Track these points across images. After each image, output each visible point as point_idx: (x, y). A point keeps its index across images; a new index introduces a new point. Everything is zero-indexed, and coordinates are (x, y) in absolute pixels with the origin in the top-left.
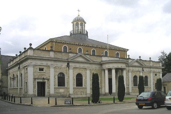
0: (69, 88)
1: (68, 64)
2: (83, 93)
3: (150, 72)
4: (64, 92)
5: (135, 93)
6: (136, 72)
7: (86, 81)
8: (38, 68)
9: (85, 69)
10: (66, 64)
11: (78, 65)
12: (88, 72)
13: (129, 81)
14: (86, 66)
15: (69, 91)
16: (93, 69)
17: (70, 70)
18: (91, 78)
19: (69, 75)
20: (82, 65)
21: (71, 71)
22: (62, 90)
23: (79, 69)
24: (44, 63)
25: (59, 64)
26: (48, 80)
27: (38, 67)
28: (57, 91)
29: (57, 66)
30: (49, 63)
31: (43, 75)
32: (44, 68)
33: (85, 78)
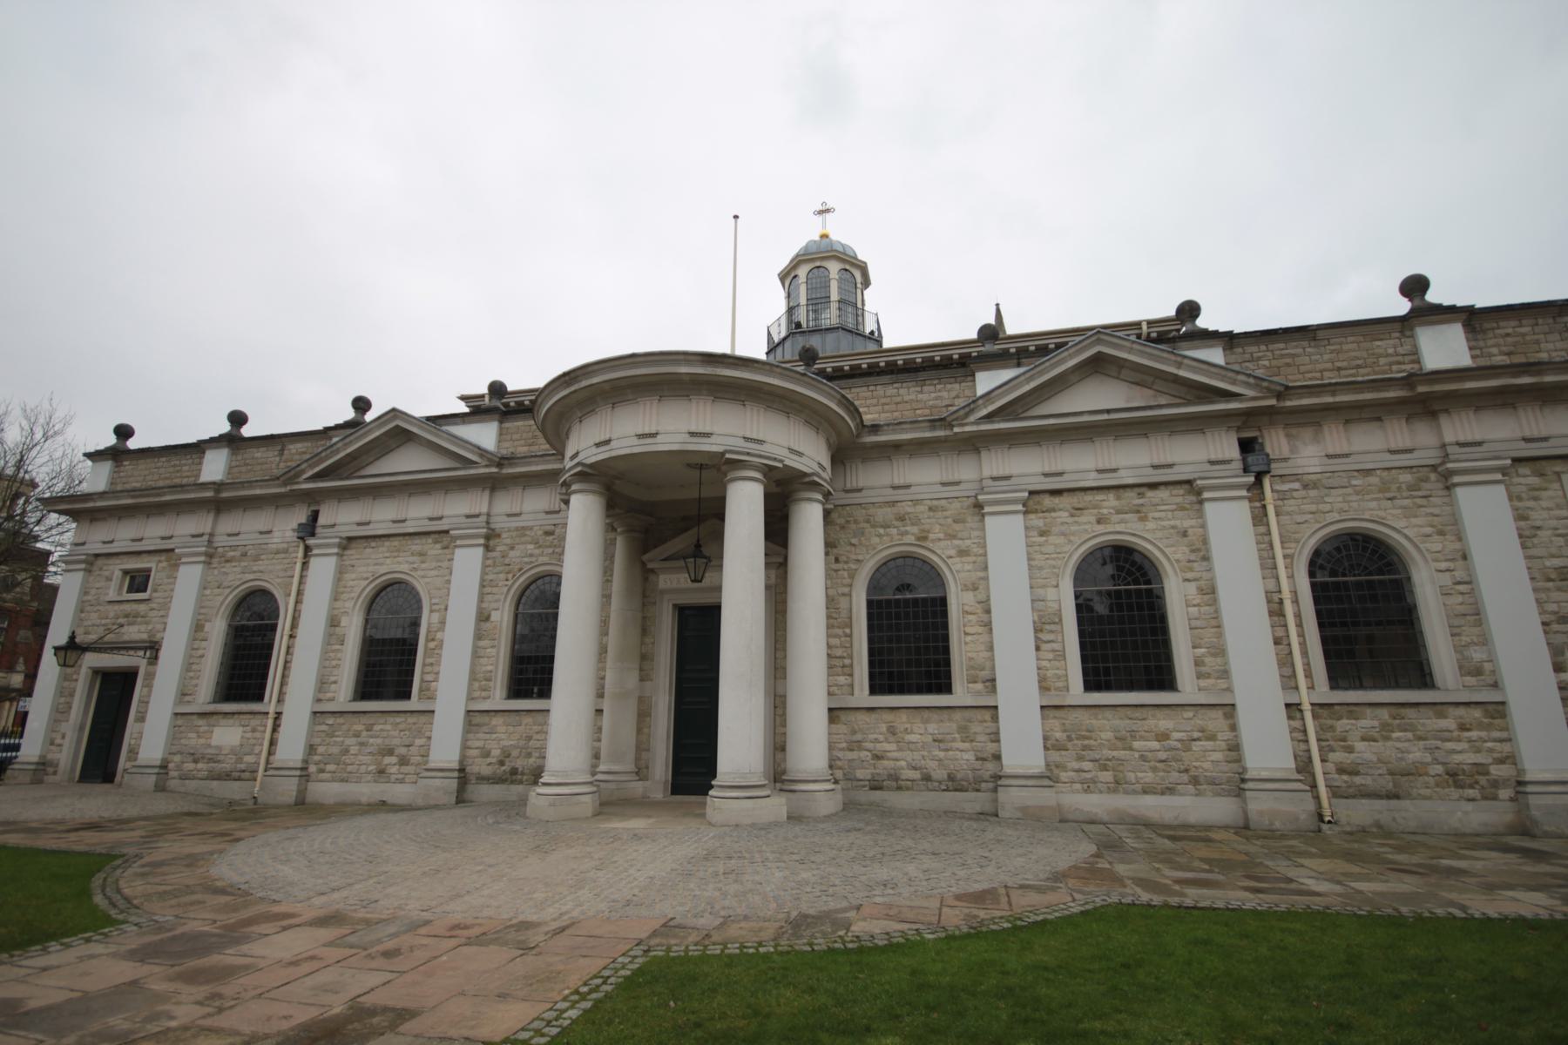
0: (279, 715)
1: (315, 516)
2: (403, 761)
3: (1444, 476)
4: (238, 753)
5: (1117, 785)
6: (1110, 501)
7: (440, 646)
8: (118, 574)
9: (442, 536)
10: (300, 516)
11: (383, 515)
12: (468, 562)
13: (988, 625)
14: (456, 508)
15: (273, 743)
16: (522, 530)
17: (313, 562)
18: (495, 616)
19: (298, 602)
20: (418, 512)
21: (323, 569)
22: (227, 736)
23: (396, 542)
24: (153, 531)
25: (247, 526)
26: (153, 648)
27: (116, 568)
28: (192, 741)
29: (233, 541)
30: (186, 527)
31: (132, 618)
32: (149, 570)
33: (435, 617)
